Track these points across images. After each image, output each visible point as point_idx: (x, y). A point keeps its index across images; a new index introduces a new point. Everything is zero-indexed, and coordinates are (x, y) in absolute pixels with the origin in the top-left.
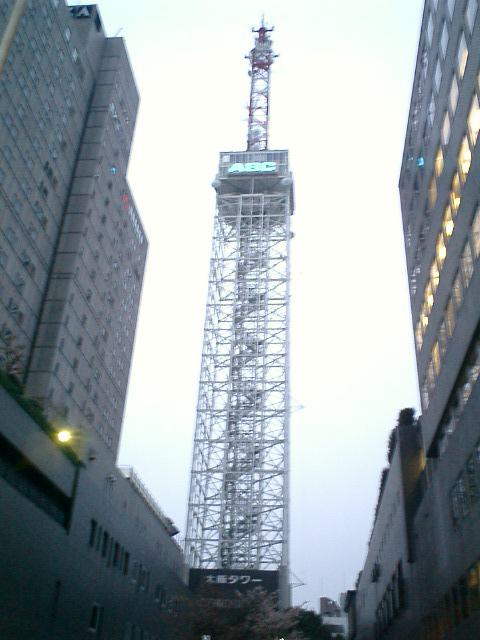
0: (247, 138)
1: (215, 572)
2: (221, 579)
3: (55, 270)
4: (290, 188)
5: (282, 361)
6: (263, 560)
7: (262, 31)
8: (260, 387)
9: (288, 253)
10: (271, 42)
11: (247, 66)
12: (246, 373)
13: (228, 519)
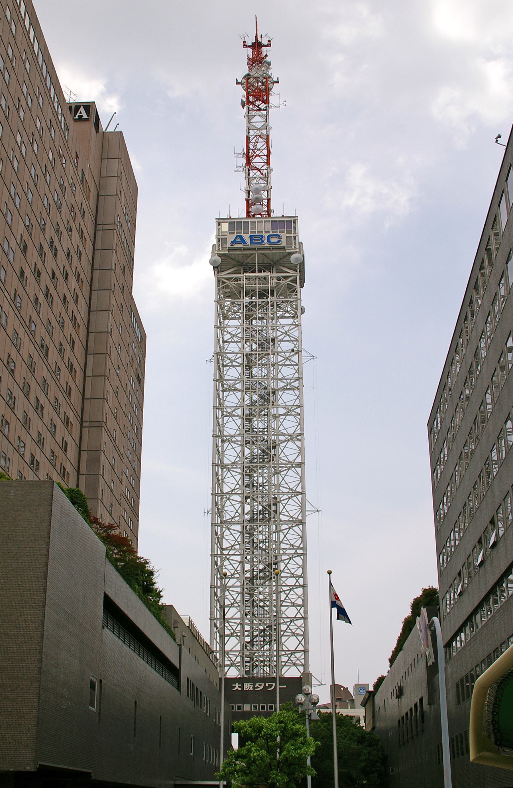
0: (244, 196)
1: (241, 681)
2: (248, 686)
3: (86, 418)
4: (301, 266)
5: (295, 358)
6: (284, 604)
7: (257, 46)
8: (272, 385)
9: (302, 518)
10: (269, 64)
11: (241, 93)
12: (258, 424)
13: (247, 567)
